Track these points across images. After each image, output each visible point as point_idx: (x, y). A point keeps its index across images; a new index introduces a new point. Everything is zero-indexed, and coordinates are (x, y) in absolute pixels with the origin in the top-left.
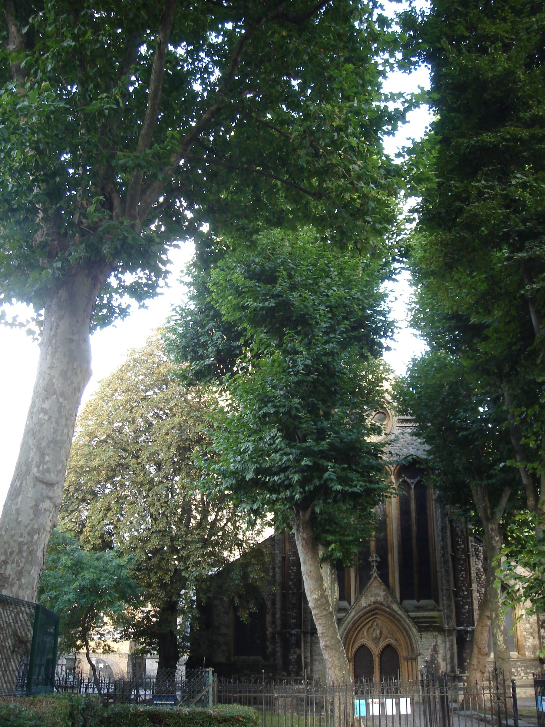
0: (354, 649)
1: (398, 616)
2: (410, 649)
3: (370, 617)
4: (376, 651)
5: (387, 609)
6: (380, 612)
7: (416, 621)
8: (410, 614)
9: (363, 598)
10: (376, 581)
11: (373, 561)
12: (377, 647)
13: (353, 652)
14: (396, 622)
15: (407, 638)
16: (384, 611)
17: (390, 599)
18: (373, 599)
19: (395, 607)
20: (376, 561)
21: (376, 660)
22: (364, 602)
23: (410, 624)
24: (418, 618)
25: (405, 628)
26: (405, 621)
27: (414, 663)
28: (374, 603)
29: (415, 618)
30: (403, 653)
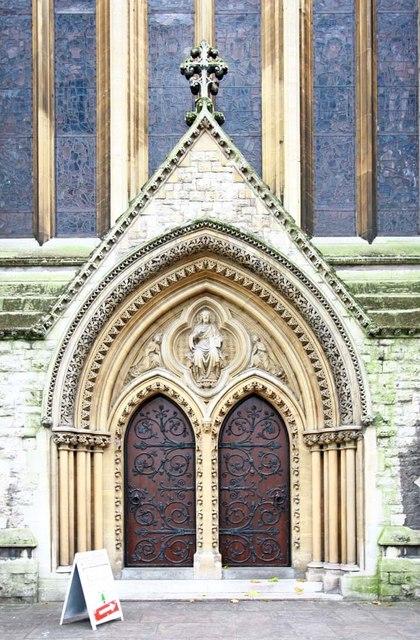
0: (124, 407)
1: (289, 276)
2: (333, 402)
3: (181, 283)
4: (205, 414)
5: (250, 250)
6: (222, 265)
7: (364, 301)
8: (342, 273)
9: (152, 207)
10: (206, 142)
11: (197, 70)
12: (207, 400)
13: (119, 416)
14: (282, 302)
15: (323, 362)
16: (234, 258)
17: (261, 207)
18: (192, 213)
19: (280, 239)
20: (212, 70)
21: (207, 447)
22: (154, 223)
23: (340, 309)
24: (374, 288)
25: (314, 324)
26: (317, 294)
27: (348, 456)
28: (199, 225)
29: (361, 289)
30: (304, 420)
